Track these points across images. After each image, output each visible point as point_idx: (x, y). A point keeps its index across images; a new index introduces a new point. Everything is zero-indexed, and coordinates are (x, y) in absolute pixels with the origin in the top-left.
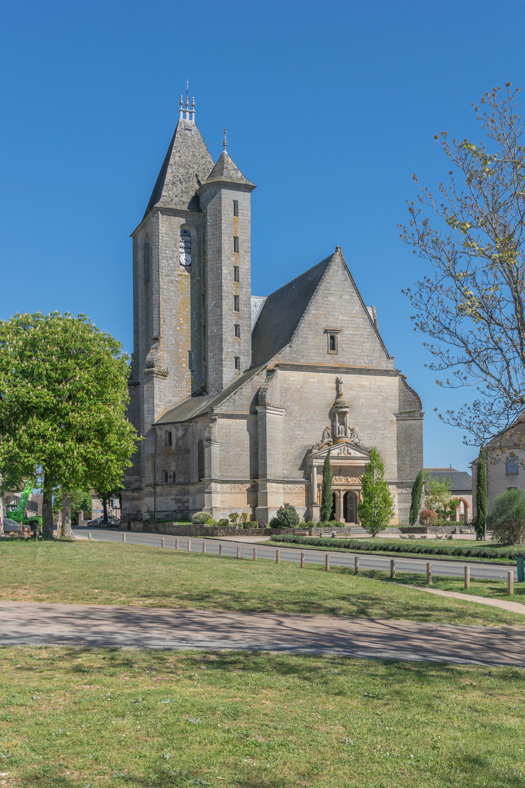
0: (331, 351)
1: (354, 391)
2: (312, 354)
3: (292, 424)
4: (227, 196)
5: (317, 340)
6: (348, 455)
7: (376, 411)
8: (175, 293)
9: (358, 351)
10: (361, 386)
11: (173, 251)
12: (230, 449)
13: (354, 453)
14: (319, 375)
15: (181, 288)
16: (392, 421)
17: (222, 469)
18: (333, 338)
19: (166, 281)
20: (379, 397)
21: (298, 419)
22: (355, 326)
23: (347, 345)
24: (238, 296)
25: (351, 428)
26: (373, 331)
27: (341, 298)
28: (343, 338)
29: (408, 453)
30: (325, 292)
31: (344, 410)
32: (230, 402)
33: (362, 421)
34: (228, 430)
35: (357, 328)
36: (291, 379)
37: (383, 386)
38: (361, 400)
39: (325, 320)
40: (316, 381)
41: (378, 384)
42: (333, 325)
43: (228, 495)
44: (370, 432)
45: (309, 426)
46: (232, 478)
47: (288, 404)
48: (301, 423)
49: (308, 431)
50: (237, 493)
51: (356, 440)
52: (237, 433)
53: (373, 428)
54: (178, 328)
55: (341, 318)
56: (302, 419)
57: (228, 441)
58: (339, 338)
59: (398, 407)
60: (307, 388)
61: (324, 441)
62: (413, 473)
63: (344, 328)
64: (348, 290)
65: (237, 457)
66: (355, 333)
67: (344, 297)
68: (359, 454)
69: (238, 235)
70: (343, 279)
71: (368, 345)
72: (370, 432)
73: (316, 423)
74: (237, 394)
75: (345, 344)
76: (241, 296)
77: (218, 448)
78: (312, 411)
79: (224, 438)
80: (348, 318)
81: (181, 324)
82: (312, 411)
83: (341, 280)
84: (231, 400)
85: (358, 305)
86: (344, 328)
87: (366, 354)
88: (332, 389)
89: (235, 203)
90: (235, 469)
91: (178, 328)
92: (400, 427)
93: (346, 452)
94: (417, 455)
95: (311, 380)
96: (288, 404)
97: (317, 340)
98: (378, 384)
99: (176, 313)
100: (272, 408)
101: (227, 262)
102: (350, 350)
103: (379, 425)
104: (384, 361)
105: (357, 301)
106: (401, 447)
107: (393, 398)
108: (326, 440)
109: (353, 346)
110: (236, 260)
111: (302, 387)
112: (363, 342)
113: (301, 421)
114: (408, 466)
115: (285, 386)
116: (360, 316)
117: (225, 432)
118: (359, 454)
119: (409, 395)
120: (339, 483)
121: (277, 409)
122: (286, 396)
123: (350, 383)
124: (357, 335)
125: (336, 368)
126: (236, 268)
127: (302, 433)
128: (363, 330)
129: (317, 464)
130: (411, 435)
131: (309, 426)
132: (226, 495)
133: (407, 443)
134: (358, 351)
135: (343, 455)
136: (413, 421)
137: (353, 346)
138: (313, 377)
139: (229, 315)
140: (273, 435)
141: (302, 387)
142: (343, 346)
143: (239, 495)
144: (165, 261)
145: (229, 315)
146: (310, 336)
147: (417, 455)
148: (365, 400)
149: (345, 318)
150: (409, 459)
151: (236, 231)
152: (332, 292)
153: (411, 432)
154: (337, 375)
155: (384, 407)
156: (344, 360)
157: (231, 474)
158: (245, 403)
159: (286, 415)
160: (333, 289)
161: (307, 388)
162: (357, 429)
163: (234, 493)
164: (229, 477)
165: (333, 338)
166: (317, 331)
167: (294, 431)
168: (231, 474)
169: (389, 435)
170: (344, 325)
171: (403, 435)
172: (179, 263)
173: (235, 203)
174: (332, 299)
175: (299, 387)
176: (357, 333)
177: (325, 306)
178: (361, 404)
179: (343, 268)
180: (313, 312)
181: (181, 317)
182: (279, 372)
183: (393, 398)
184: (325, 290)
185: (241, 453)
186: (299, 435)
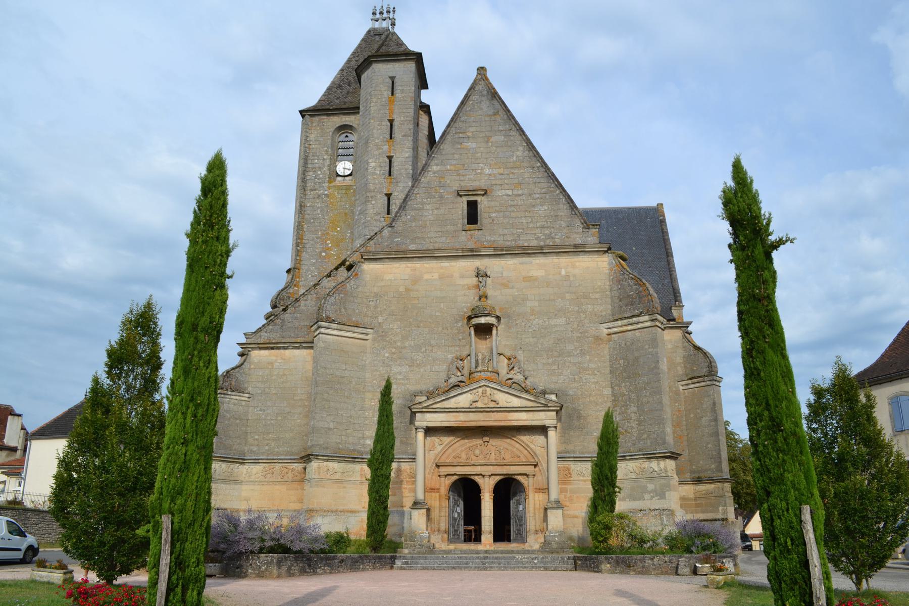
0: (472, 226)
1: (513, 288)
2: (433, 235)
3: (387, 355)
4: (380, 71)
5: (442, 211)
6: (492, 405)
7: (561, 321)
8: (322, 210)
9: (524, 221)
10: (528, 279)
11: (324, 159)
12: (269, 403)
13: (504, 399)
14: (442, 268)
15: (332, 203)
16: (597, 339)
17: (250, 440)
18: (472, 207)
19: (311, 196)
20: (568, 296)
21: (399, 344)
22: (516, 181)
23: (501, 214)
24: (391, 194)
25: (508, 354)
26: (553, 185)
27: (487, 142)
28: (493, 204)
29: (633, 396)
30: (456, 136)
31: (483, 320)
32: (276, 324)
33: (532, 340)
34: (267, 372)
35: (520, 184)
36: (388, 277)
37: (574, 276)
38: (529, 304)
39: (457, 178)
40: (436, 276)
41: (563, 272)
42: (471, 182)
43: (257, 487)
44: (550, 361)
45: (419, 357)
46: (268, 455)
47: (380, 319)
48: (404, 351)
49: (419, 365)
50: (274, 483)
51: (519, 377)
52: (284, 375)
53: (555, 354)
54: (324, 254)
55: (487, 171)
56: (407, 344)
57: (267, 390)
58: (483, 203)
59: (609, 312)
60: (417, 291)
61: (451, 381)
62: (645, 436)
63: (494, 187)
64: (501, 128)
65: (280, 418)
66: (516, 192)
67: (493, 139)
68: (516, 402)
69: (395, 117)
70: (491, 112)
71: (542, 210)
72: (550, 361)
73: (435, 350)
74: (288, 311)
75: (496, 211)
76: (395, 194)
77: (244, 403)
78: (427, 330)
79: (259, 385)
80: (501, 171)
81: (329, 249)
82: (427, 330)
83: (487, 115)
84: (278, 322)
85: (521, 148)
86: (494, 187)
87: (538, 224)
88: (469, 288)
89: (393, 79)
90: (274, 440)
91: (324, 254)
92: (614, 349)
93: (486, 400)
94: (650, 399)
95: (427, 276)
96: (380, 319)
97: (442, 211)
98: (563, 272)
99: (322, 235)
100: (335, 326)
101: (376, 152)
102: (506, 221)
103: (570, 347)
104: (577, 233)
105: (518, 142)
106: (619, 385)
107: (597, 296)
108: (453, 380)
109: (513, 214)
110: (390, 148)
111: (407, 290)
112: (534, 206)
113: (405, 347)
114: (634, 424)
115: (375, 289)
116: (525, 164)
117: (263, 376)
118: (516, 402)
119: (629, 285)
120: (482, 462)
121: (356, 330)
122: (376, 307)
123: (505, 274)
124: (520, 195)
125: (472, 250)
126: (390, 158)
127: (405, 369)
128: (532, 186)
129: (425, 424)
130: (637, 359)
131: (419, 357)
132: (252, 487)
133: (629, 377)
134: (524, 221)
135: (479, 405)
136: (637, 333)
137: (513, 214)
138: (430, 270)
139: (376, 220)
140: (338, 373)
141: (407, 290)
142: (494, 215)
143: (277, 487)
144: (311, 173)
145: (376, 220)
146: (428, 207)
147: (650, 399)
148: (536, 304)
149: (495, 171)
150: (635, 409)
151: (391, 111)
152: (470, 134)
153: (636, 354)
154: (477, 263)
155: (578, 312)
156: (495, 238)
157: (267, 448)
158: (302, 324)
159: (374, 340)
160: (471, 130)
161: (417, 291)
162: (521, 356)
163: (268, 483)
164: (263, 454)
165: (472, 207)
166: (442, 197)
167: (390, 366)
168: (267, 448)
169: (592, 366)
170: (494, 182)
171: (622, 362)
172: (334, 174)
173: (393, 79)
174: (471, 145)
175: (402, 289)
176: (520, 192)
177: (456, 156)
178: (529, 310)
179: (490, 97)
180: (435, 168)
181: (329, 239)
182: (367, 267)
183: (597, 296)
184: (456, 133)
185: (287, 410)
186: (400, 373)
